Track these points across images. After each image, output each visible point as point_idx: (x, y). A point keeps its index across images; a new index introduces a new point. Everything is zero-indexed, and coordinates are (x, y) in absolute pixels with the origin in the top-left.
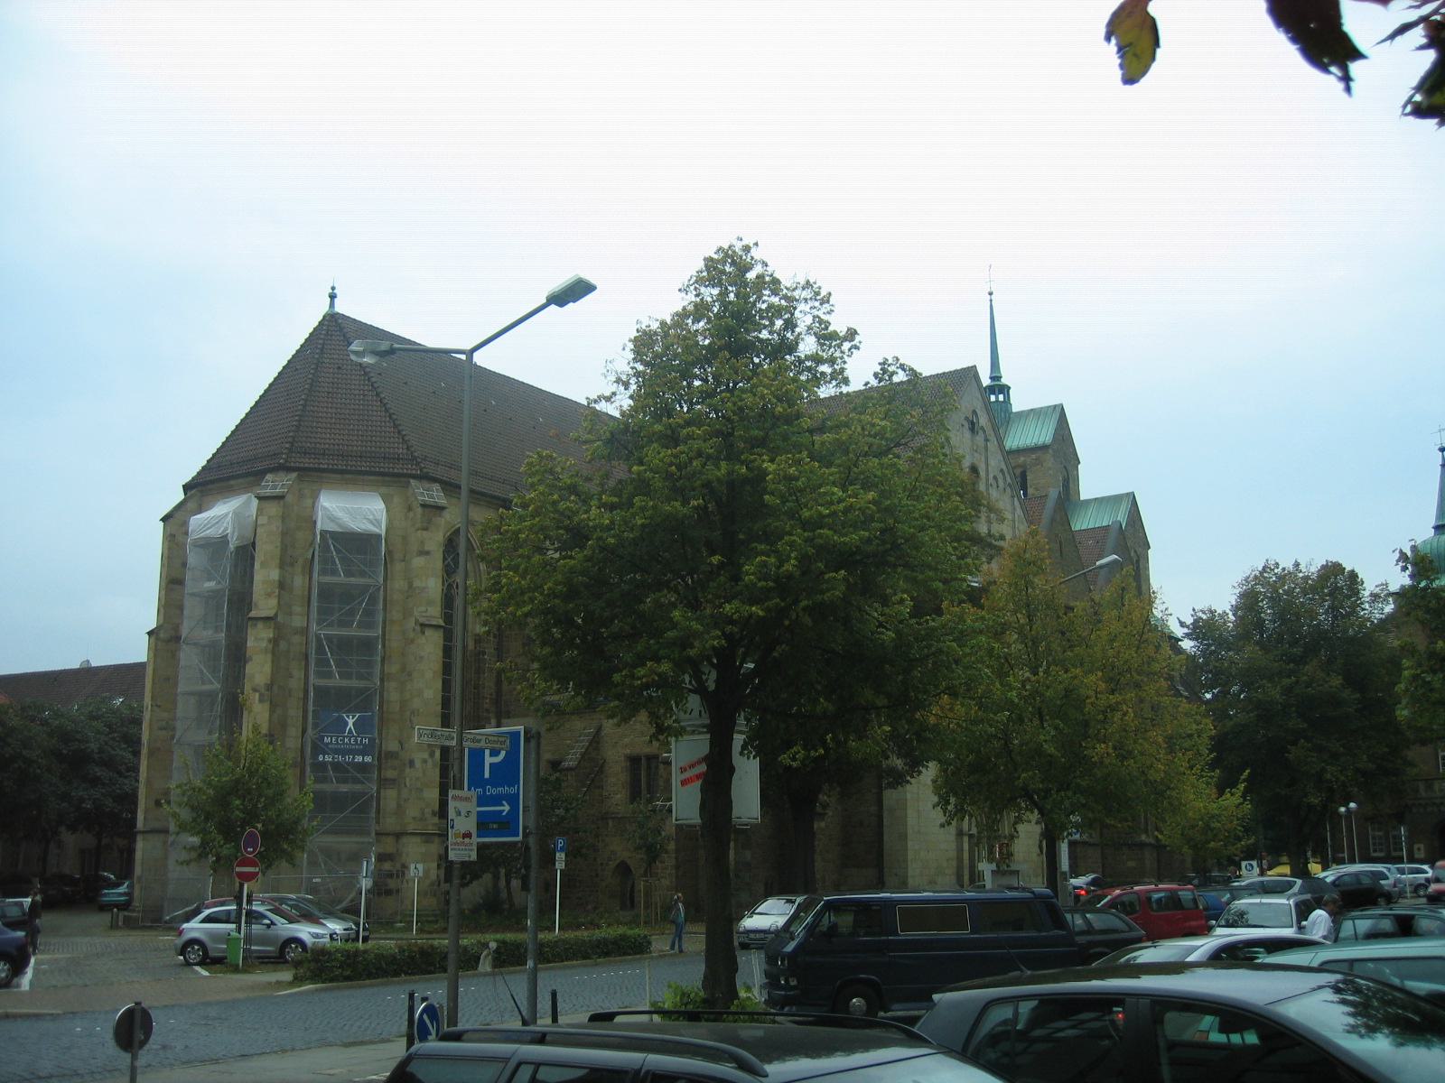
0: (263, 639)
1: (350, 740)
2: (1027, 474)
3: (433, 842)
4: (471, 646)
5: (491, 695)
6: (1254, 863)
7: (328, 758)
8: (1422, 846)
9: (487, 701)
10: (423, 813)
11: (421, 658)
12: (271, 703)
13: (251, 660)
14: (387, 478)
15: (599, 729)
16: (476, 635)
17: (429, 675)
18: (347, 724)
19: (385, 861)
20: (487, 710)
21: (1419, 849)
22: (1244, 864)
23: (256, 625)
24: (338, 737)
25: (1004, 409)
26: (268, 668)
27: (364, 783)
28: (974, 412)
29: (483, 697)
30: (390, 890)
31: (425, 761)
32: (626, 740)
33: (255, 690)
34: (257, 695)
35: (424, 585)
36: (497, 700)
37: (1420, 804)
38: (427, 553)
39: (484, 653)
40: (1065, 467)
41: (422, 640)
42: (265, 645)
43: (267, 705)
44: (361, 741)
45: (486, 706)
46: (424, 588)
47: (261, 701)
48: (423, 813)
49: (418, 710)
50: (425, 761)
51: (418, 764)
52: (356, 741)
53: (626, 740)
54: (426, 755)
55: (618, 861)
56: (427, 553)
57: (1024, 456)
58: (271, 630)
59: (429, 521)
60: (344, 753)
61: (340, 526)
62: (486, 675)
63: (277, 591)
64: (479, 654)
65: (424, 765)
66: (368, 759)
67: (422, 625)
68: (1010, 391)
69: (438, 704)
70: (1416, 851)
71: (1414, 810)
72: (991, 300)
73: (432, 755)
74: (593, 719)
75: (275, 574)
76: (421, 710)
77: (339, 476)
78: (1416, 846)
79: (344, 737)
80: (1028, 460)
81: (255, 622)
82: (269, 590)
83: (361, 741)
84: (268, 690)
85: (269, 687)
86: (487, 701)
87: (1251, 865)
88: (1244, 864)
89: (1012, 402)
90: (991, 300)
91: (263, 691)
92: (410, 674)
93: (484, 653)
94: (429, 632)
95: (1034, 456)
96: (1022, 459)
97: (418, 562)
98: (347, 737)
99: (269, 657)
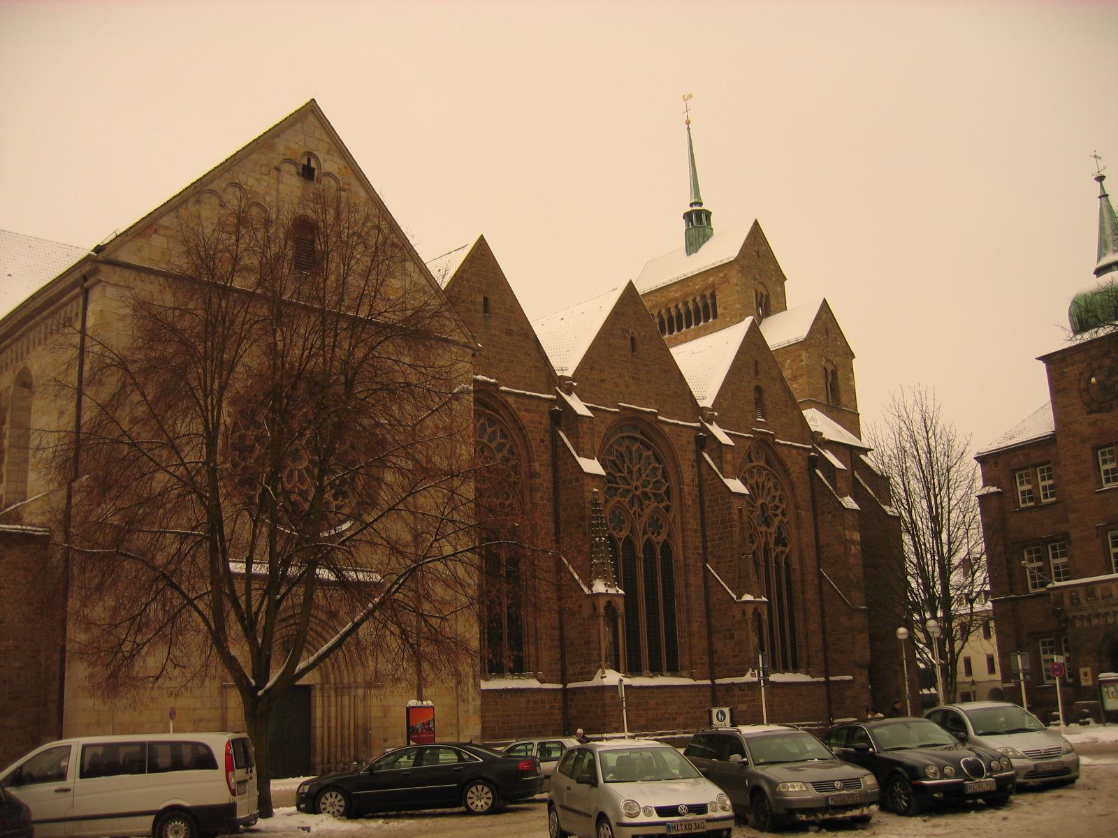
2: (717, 293)
6: (726, 710)
8: (1088, 669)
21: (1086, 674)
22: (715, 711)
25: (702, 233)
28: (310, 155)
37: (1083, 616)
40: (761, 283)
57: (712, 276)
68: (712, 218)
70: (1082, 677)
71: (1078, 624)
72: (689, 129)
78: (1082, 670)
80: (717, 279)
87: (723, 713)
88: (715, 711)
89: (713, 226)
90: (689, 129)
95: (721, 275)
96: (711, 279)
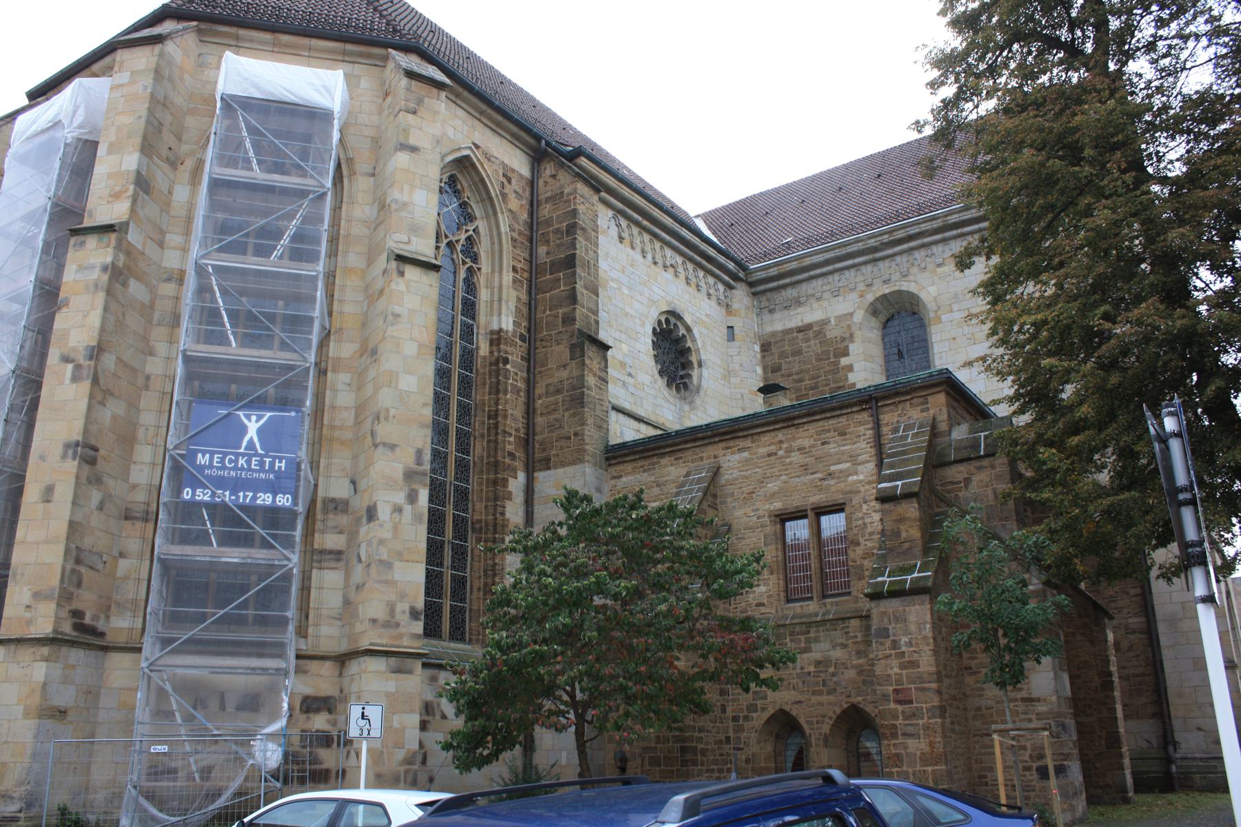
0: (93, 267)
1: (249, 462)
3: (410, 672)
4: (484, 349)
5: (517, 430)
7: (203, 496)
9: (512, 439)
10: (392, 612)
11: (397, 316)
12: (95, 381)
13: (67, 304)
14: (349, 47)
15: (716, 472)
16: (492, 332)
17: (410, 349)
18: (244, 430)
19: (317, 710)
20: (511, 455)
23: (83, 243)
24: (225, 454)
26: (95, 319)
27: (273, 547)
29: (504, 432)
30: (327, 771)
31: (398, 510)
32: (772, 486)
33: (66, 359)
34: (70, 367)
35: (406, 199)
36: (527, 442)
38: (414, 149)
39: (506, 361)
41: (398, 285)
42: (96, 276)
43: (85, 386)
44: (272, 464)
45: (509, 448)
46: (405, 205)
47: (75, 379)
48: (392, 612)
49: (387, 410)
50: (398, 510)
51: (384, 512)
52: (262, 463)
53: (772, 486)
54: (400, 497)
55: (771, 711)
56: (414, 149)
58: (110, 250)
59: (420, 102)
60: (236, 485)
61: (255, 86)
62: (508, 396)
63: (132, 187)
64: (497, 362)
65: (396, 515)
66: (284, 500)
67: (401, 259)
69: (425, 405)
73: (412, 498)
74: (701, 459)
75: (131, 161)
76: (392, 412)
77: (267, 36)
79: (237, 455)
81: (81, 238)
82: (118, 188)
83: (272, 464)
84: (91, 358)
85: (96, 352)
86: (512, 439)
91: (81, 360)
92: (374, 352)
93: (506, 361)
94: (412, 272)
97: (402, 159)
98: (243, 455)
99: (101, 297)
